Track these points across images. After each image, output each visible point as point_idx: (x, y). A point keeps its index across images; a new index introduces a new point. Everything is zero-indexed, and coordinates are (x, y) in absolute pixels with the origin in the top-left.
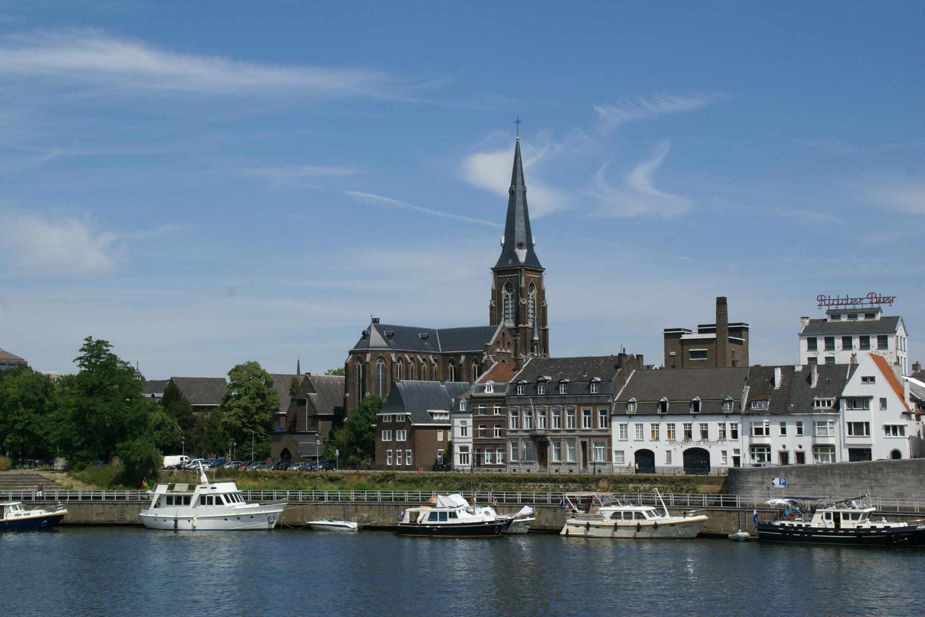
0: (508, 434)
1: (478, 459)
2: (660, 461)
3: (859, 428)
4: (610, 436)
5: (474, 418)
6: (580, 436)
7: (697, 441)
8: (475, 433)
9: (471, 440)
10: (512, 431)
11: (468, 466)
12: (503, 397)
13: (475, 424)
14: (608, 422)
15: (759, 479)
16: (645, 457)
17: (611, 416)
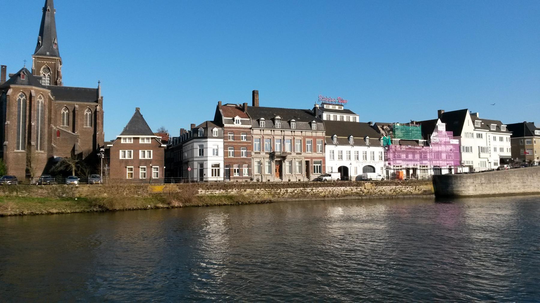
0: (253, 154)
1: (228, 174)
2: (353, 174)
3: (438, 155)
4: (324, 158)
5: (224, 142)
6: (305, 158)
7: (369, 162)
8: (226, 154)
9: (222, 159)
10: (256, 153)
11: (221, 178)
12: (251, 128)
13: (225, 147)
14: (323, 150)
15: (472, 180)
16: (344, 170)
17: (325, 144)
